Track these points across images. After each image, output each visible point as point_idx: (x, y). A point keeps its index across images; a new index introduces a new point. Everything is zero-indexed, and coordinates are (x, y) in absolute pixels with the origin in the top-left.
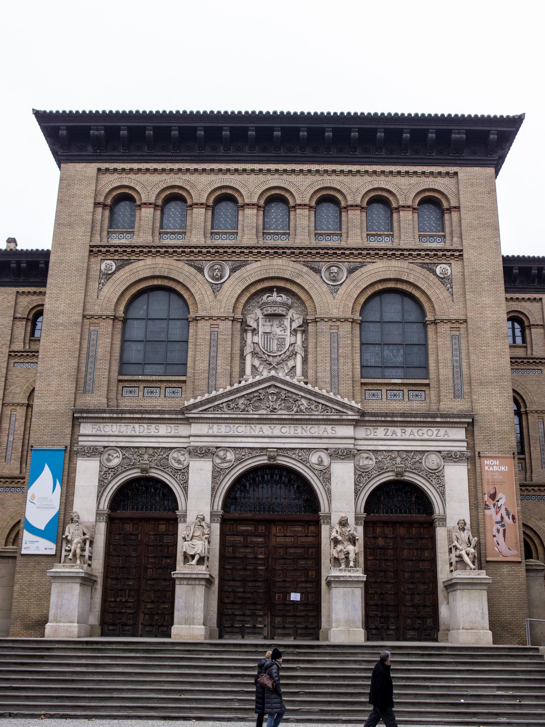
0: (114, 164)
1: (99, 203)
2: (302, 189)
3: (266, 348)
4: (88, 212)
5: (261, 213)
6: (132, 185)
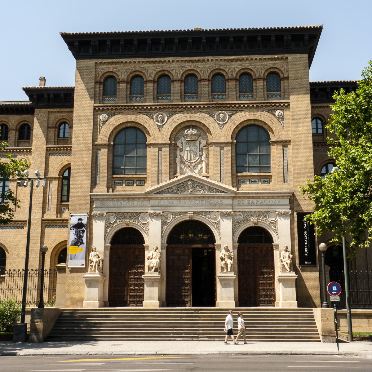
0: (104, 60)
1: (97, 82)
2: (204, 70)
4: (92, 87)
5: (183, 84)
6: (114, 71)
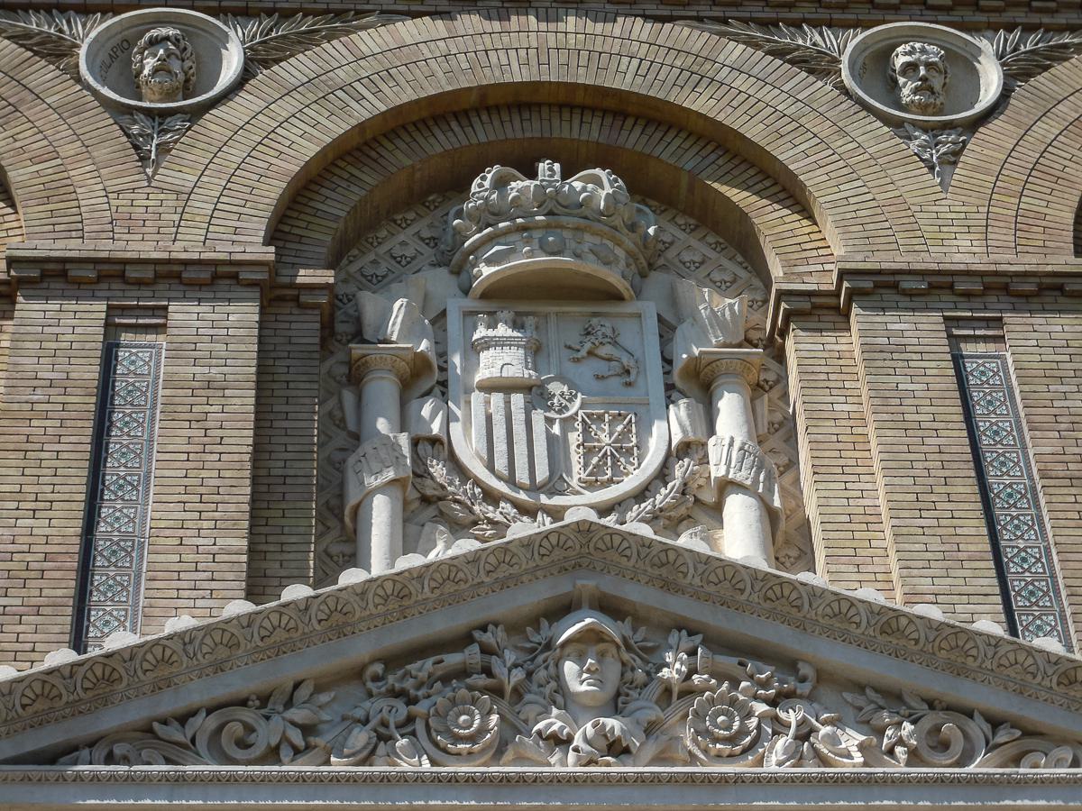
3: (501, 464)
